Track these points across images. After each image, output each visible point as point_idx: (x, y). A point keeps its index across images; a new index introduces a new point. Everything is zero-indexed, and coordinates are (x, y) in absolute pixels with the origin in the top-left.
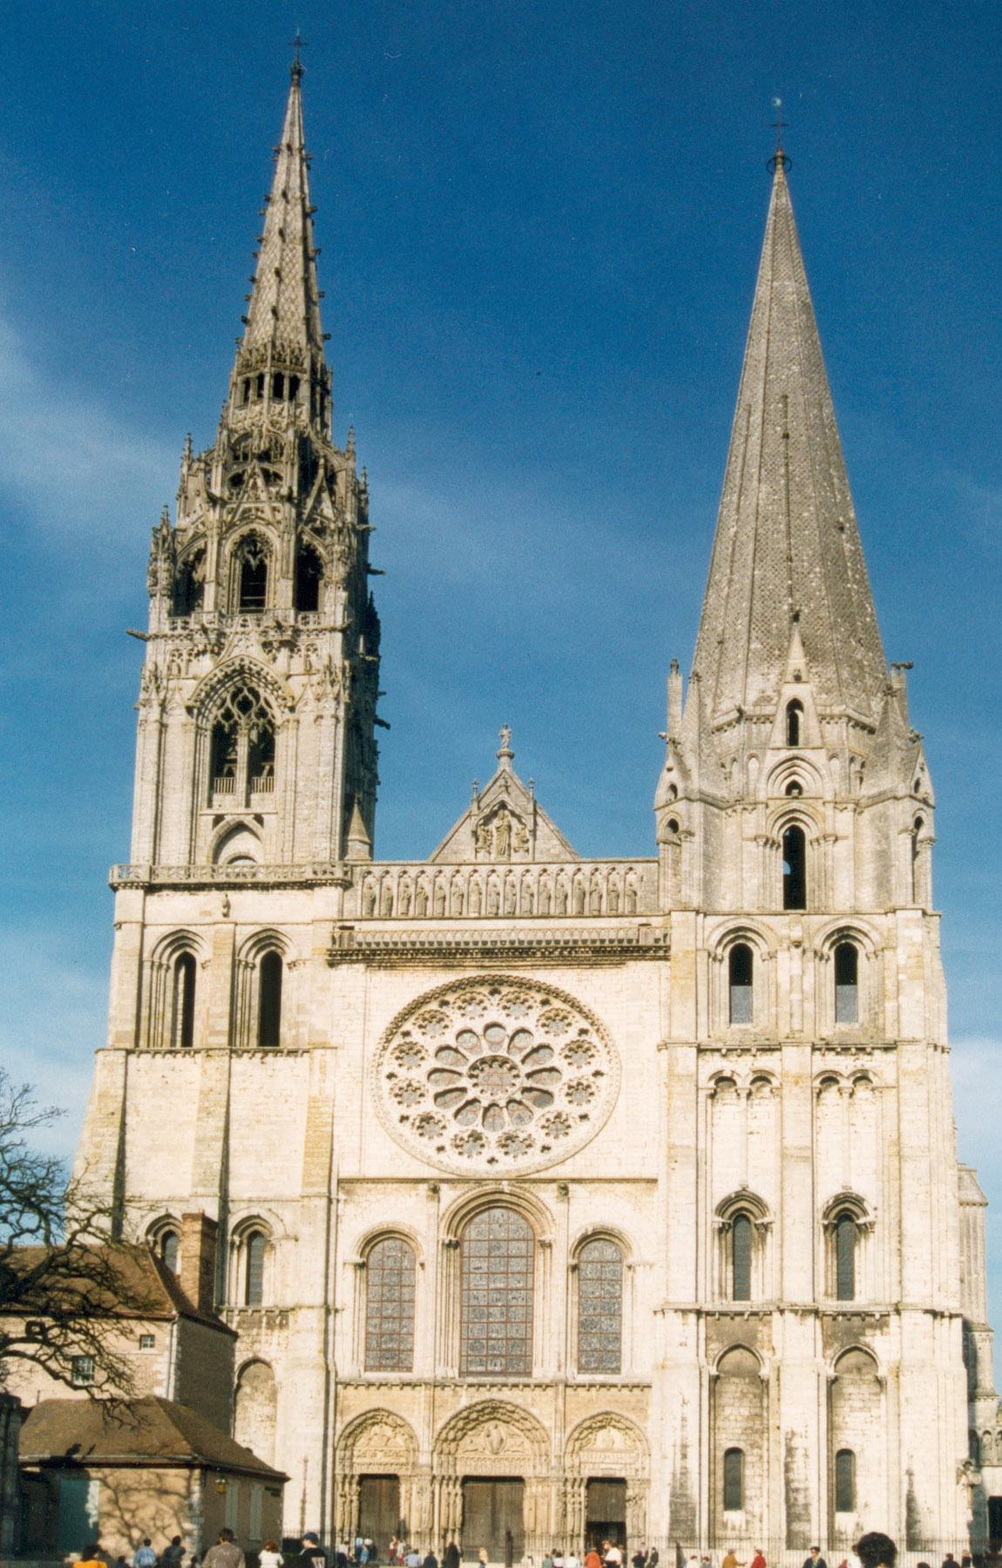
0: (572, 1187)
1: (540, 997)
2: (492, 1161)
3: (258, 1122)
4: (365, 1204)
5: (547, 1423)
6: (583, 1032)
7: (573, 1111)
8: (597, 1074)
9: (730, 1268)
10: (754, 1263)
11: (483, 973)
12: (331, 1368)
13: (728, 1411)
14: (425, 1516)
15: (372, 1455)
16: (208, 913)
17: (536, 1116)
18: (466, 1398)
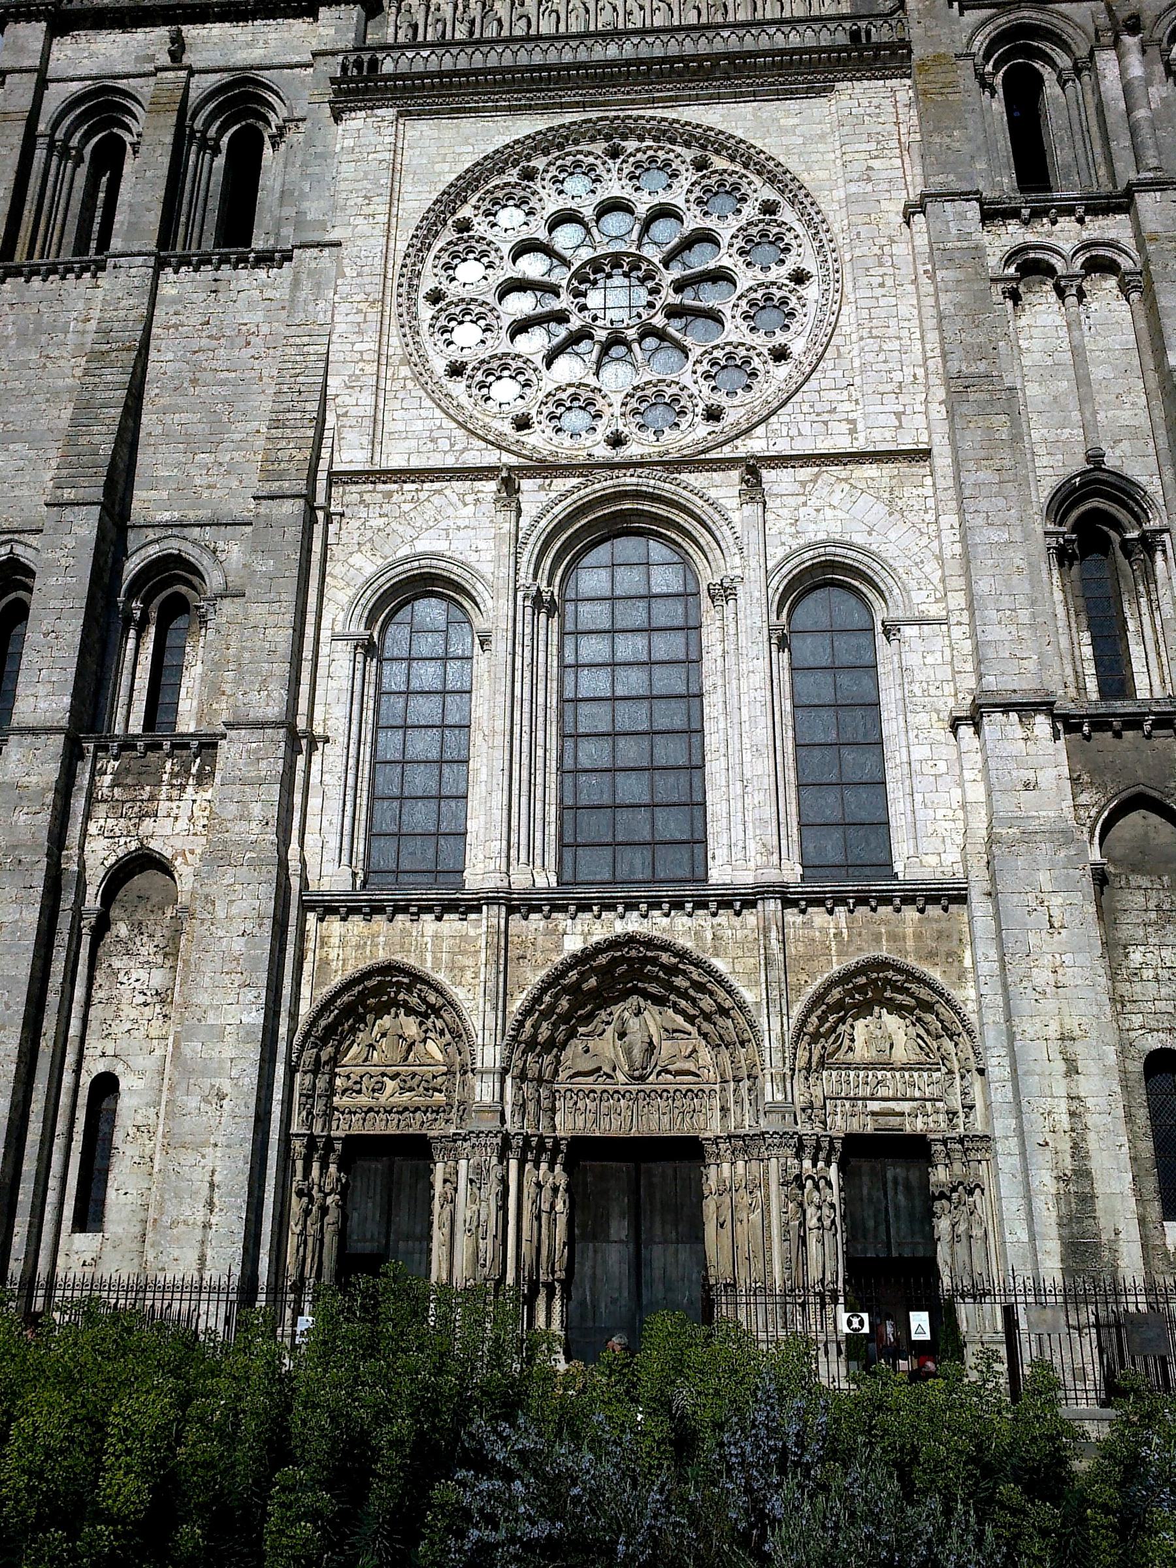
0: (767, 475)
1: (689, 154)
2: (616, 441)
3: (194, 382)
4: (381, 522)
5: (749, 996)
6: (769, 208)
7: (758, 340)
8: (800, 277)
9: (1086, 637)
10: (1132, 625)
11: (594, 115)
12: (294, 864)
13: (1136, 957)
14: (487, 1246)
15: (375, 1085)
16: (151, 58)
17: (692, 358)
18: (578, 934)
